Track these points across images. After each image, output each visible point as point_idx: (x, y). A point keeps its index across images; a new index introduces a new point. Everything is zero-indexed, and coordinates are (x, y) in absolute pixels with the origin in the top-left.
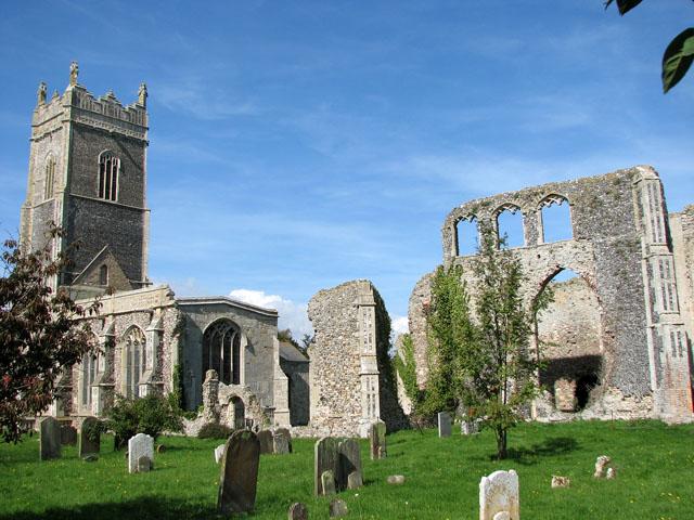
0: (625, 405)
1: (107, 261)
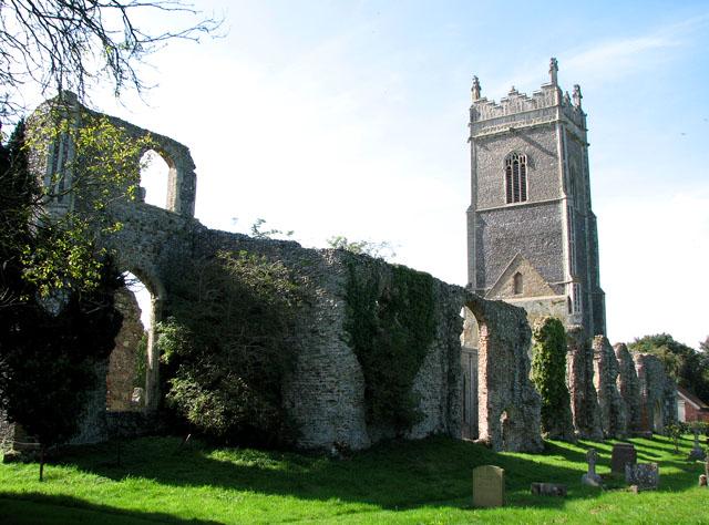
1: (521, 268)
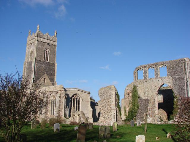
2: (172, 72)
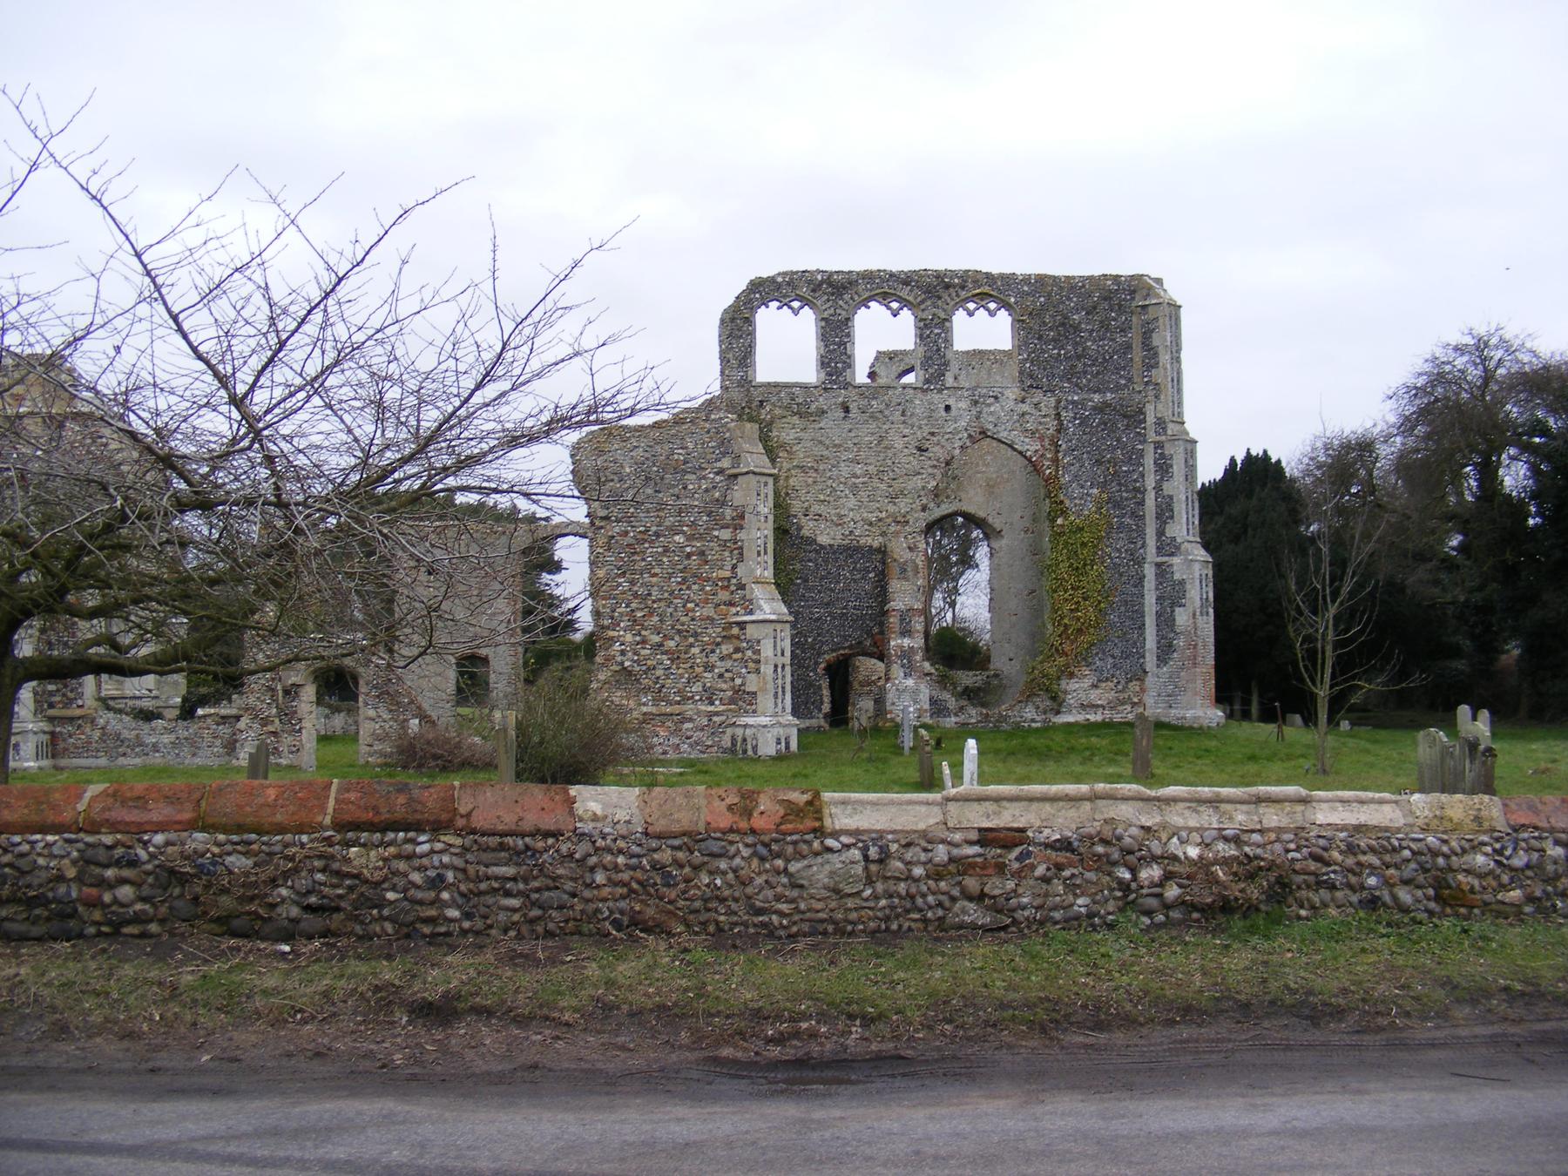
0: (1095, 696)
2: (1057, 358)
